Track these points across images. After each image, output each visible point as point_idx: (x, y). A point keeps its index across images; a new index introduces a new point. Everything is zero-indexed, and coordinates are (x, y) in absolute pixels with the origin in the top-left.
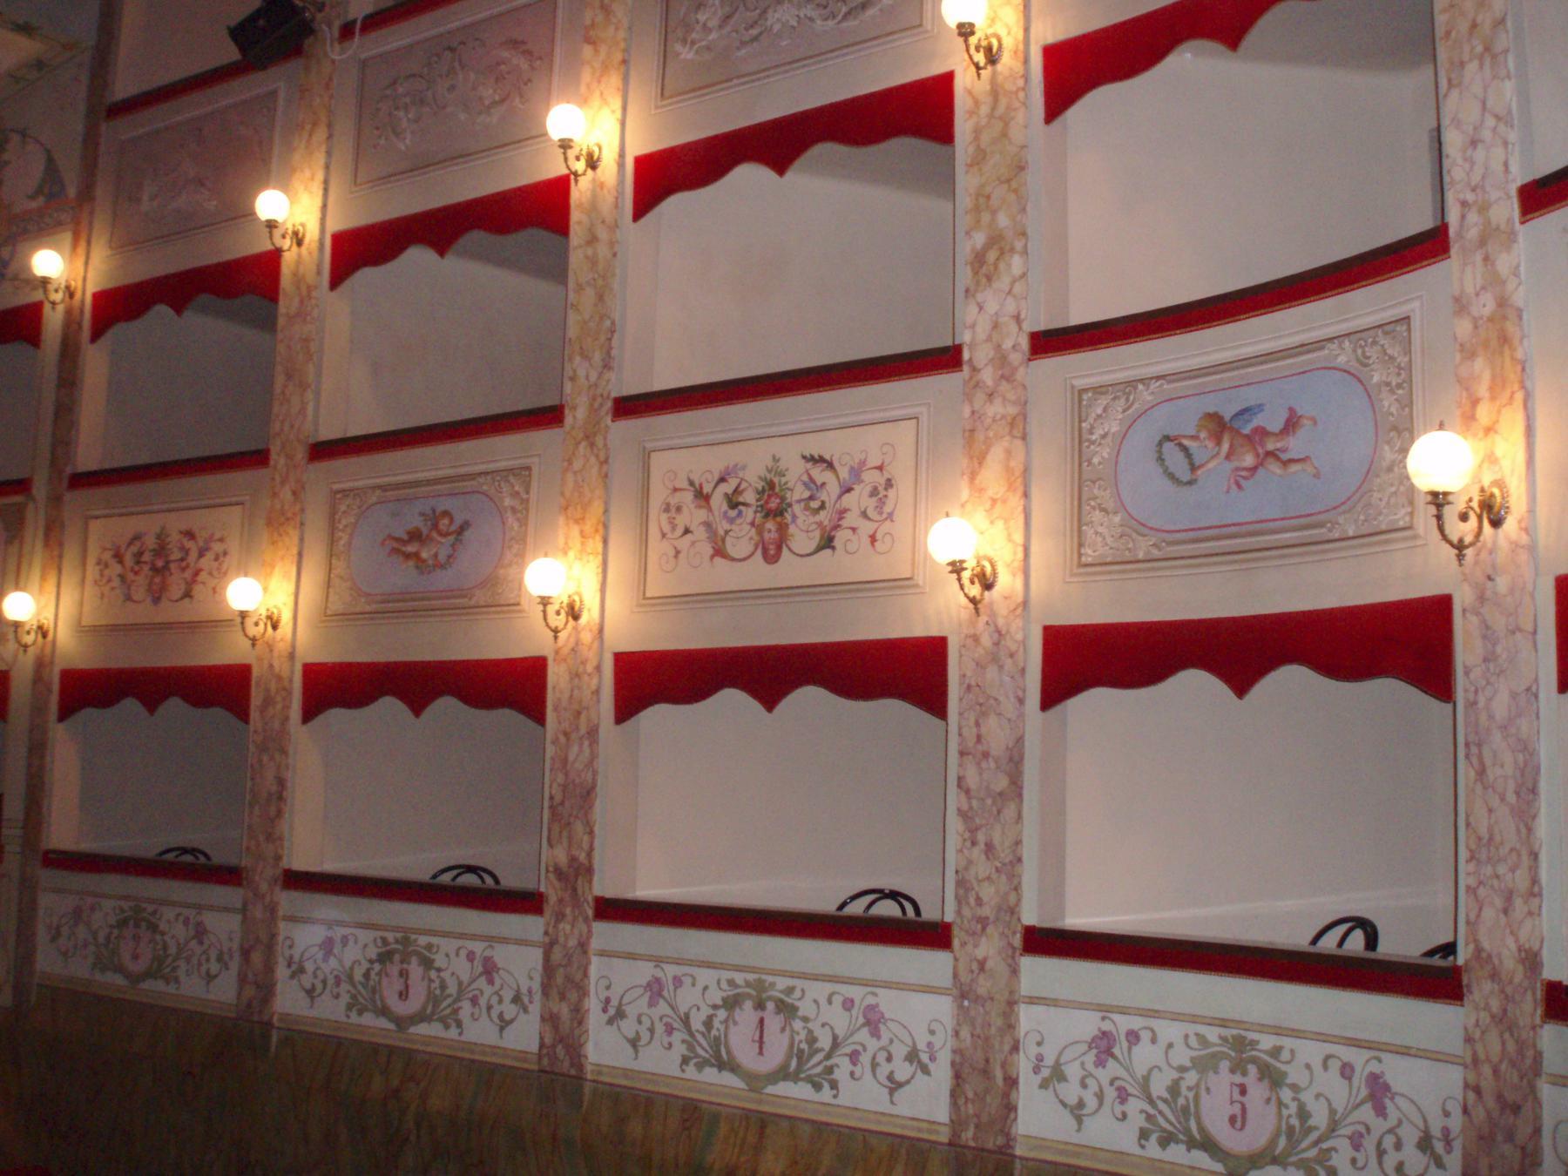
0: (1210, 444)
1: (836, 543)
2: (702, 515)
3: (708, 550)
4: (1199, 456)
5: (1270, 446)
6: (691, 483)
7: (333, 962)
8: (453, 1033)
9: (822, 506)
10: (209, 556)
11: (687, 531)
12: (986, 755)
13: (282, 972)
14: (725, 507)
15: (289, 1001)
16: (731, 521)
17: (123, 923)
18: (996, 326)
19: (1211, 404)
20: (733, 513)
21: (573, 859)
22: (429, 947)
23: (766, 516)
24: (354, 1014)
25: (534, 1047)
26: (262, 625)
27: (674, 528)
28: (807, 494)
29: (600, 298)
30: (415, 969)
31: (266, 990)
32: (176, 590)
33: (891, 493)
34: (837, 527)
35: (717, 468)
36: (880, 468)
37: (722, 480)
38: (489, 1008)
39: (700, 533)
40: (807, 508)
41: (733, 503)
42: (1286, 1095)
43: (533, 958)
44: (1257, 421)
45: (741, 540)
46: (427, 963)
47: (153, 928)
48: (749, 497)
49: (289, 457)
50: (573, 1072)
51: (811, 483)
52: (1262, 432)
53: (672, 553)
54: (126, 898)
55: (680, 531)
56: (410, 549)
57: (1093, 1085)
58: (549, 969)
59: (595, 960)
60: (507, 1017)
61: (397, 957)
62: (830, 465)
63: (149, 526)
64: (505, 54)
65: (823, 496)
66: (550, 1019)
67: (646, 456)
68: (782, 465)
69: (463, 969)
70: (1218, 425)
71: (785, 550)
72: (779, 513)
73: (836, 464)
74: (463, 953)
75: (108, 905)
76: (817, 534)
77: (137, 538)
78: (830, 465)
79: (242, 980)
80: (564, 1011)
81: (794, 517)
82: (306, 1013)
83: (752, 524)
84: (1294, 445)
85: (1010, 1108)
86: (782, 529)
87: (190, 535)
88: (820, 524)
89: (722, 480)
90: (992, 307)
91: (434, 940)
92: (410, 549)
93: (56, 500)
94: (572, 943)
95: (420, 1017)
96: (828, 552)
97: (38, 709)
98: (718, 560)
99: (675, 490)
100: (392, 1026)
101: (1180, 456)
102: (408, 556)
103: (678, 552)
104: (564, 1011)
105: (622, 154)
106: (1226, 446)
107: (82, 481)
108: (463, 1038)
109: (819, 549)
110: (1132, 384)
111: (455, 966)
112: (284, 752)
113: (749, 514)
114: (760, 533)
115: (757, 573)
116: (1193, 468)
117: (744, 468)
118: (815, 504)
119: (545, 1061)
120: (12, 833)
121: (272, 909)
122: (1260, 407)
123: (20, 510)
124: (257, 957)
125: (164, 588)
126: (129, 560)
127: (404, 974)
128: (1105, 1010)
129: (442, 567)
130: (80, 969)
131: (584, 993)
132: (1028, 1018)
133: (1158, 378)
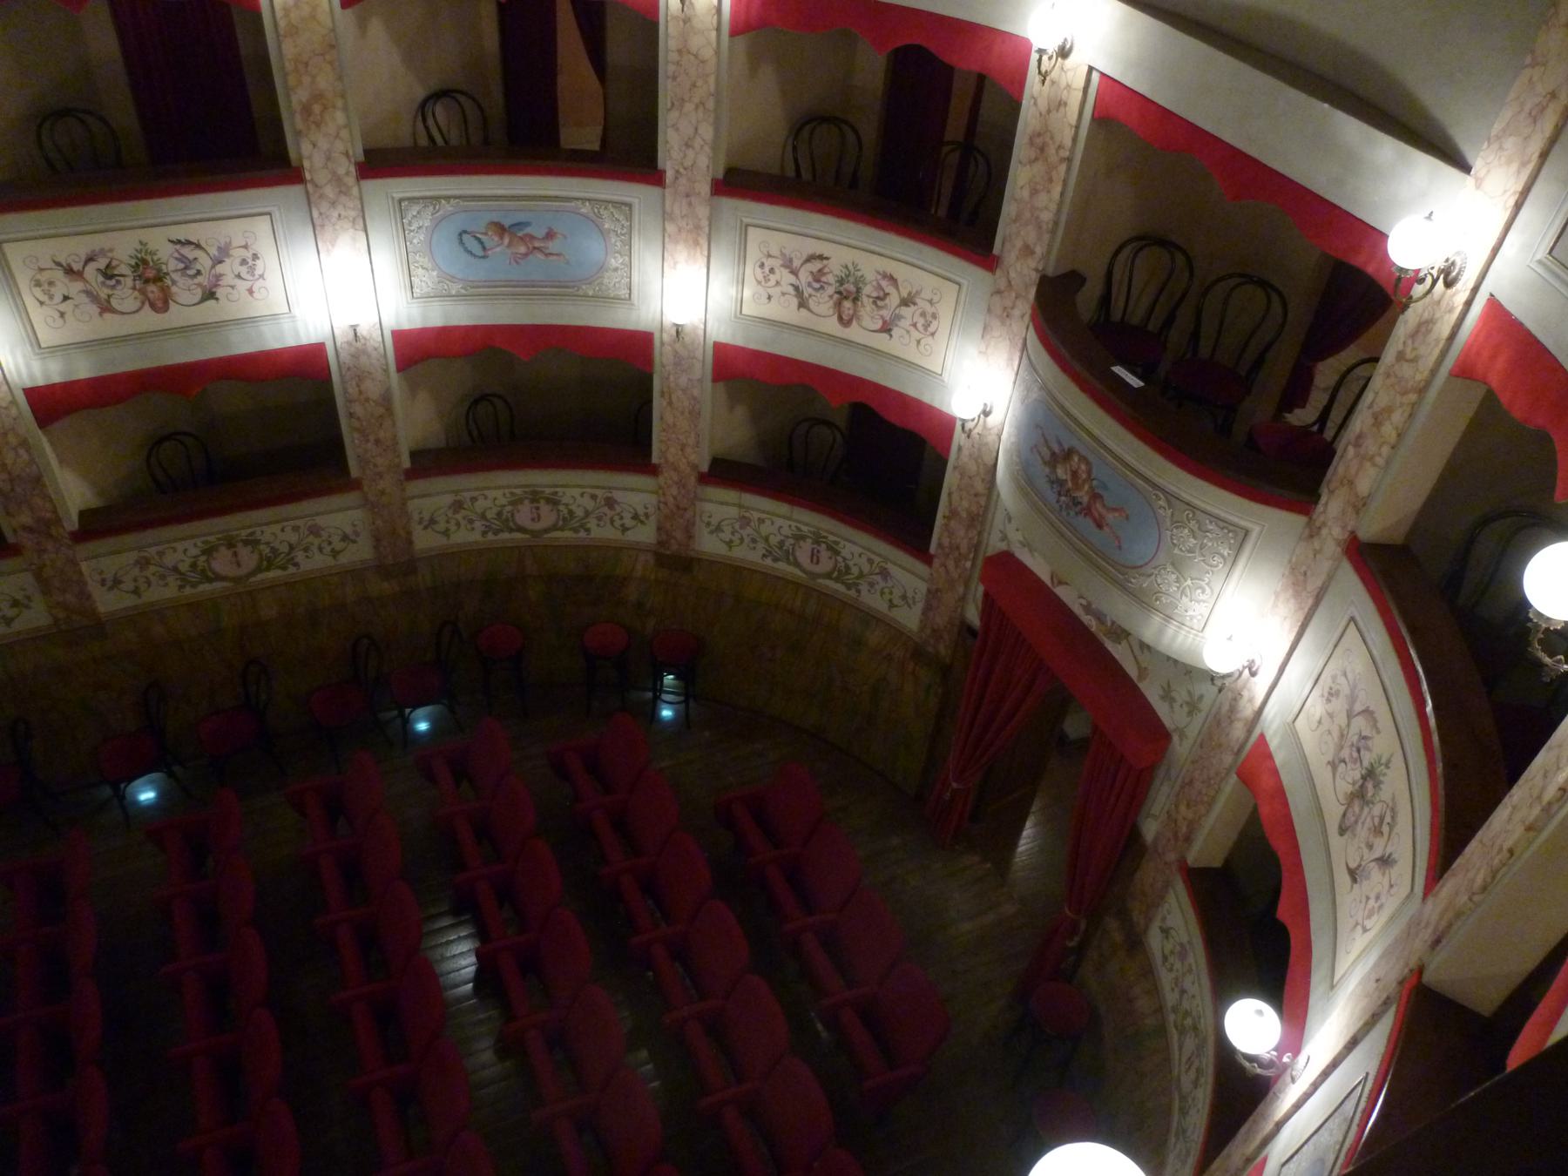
0: (496, 239)
2: (79, 285)
3: (94, 309)
4: (487, 245)
5: (537, 244)
6: (59, 264)
9: (199, 272)
11: (66, 298)
12: (367, 400)
14: (101, 279)
16: (113, 287)
18: (329, 158)
19: (495, 217)
23: (147, 281)
27: (51, 297)
34: (217, 286)
35: (83, 253)
36: (246, 247)
37: (90, 259)
39: (84, 299)
41: (108, 274)
42: (561, 508)
44: (528, 230)
45: (125, 297)
51: (182, 259)
52: (532, 238)
53: (57, 315)
55: (58, 298)
57: (453, 522)
62: (198, 246)
65: (198, 267)
68: (151, 247)
70: (500, 229)
72: (159, 278)
73: (203, 244)
76: (199, 292)
78: (198, 246)
81: (174, 282)
83: (134, 288)
84: (553, 246)
85: (410, 542)
88: (199, 285)
89: (90, 259)
90: (323, 144)
96: (211, 303)
98: (108, 316)
99: (41, 270)
101: (475, 243)
103: (62, 315)
104: (70, 598)
106: (506, 241)
109: (203, 300)
110: (438, 198)
114: (143, 292)
115: (149, 320)
116: (484, 248)
117: (111, 250)
122: (527, 224)
128: (456, 492)
132: (412, 505)
133: (459, 197)
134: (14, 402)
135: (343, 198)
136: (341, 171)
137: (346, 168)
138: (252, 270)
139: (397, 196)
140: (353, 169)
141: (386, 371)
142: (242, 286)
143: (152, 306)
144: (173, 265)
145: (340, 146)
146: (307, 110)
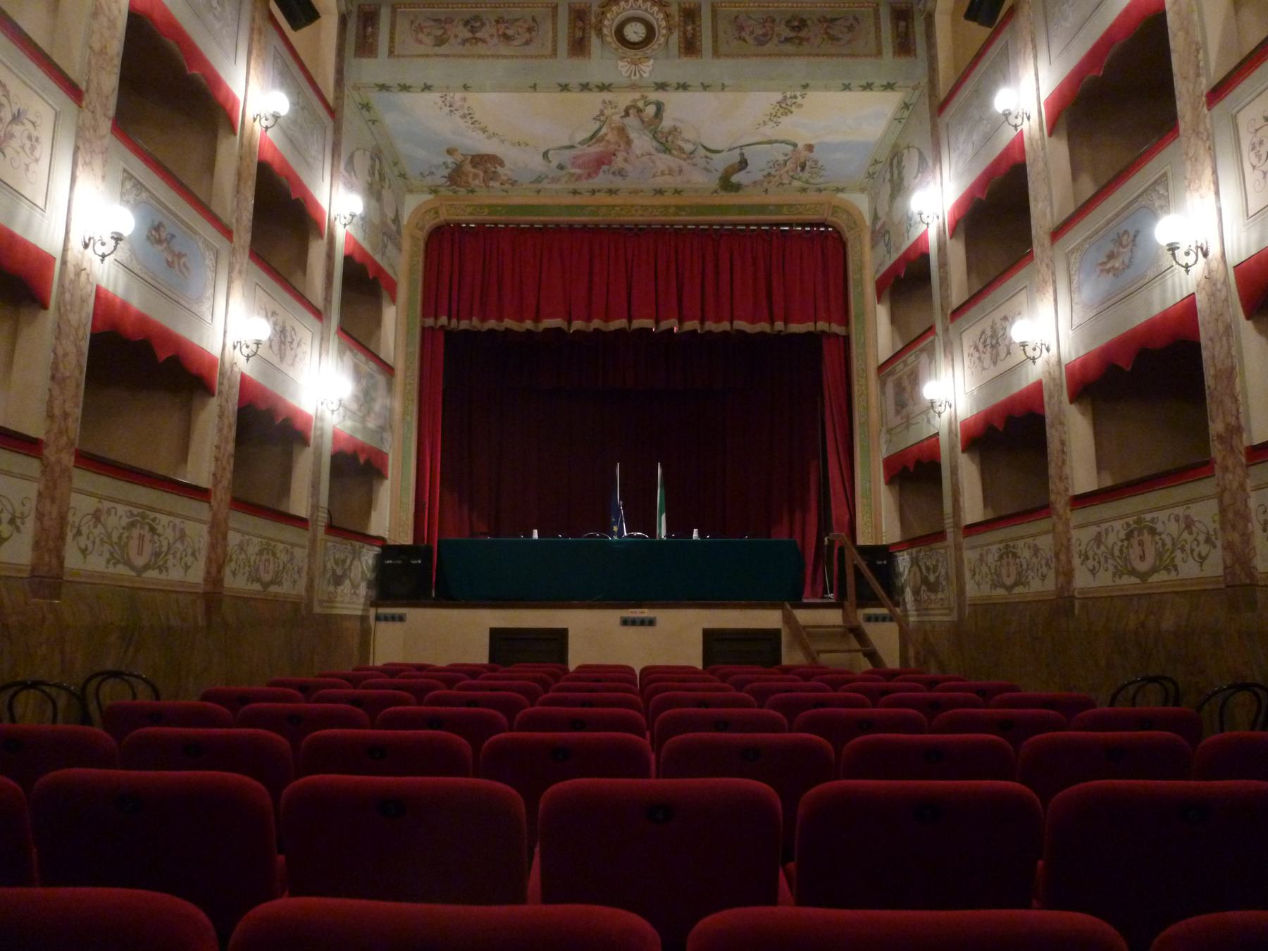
7: (1102, 547)
8: (1173, 575)
13: (1076, 561)
15: (1082, 580)
17: (1001, 558)
21: (1227, 425)
22: (1153, 520)
24: (1117, 579)
25: (1220, 571)
26: (1038, 350)
29: (1187, 33)
30: (1147, 537)
31: (1068, 575)
32: (1003, 354)
38: (1192, 551)
43: (1213, 506)
46: (1153, 531)
47: (1015, 555)
49: (1043, 246)
50: (1248, 581)
54: (1001, 542)
56: (1109, 266)
58: (1223, 511)
59: (1253, 494)
60: (1204, 554)
61: (1136, 533)
63: (985, 324)
66: (1229, 546)
67: (1234, 118)
69: (1173, 528)
74: (1172, 518)
75: (994, 548)
77: (983, 333)
79: (1057, 573)
80: (1235, 537)
82: (1093, 584)
91: (1154, 515)
92: (1109, 266)
93: (946, 330)
94: (1235, 484)
95: (1154, 570)
100: (1138, 581)
102: (1108, 271)
104: (1235, 537)
107: (957, 313)
108: (1180, 576)
111: (1169, 526)
112: (1062, 423)
119: (1229, 578)
120: (949, 522)
121: (1067, 524)
123: (933, 342)
124: (1063, 557)
125: (998, 354)
126: (981, 347)
127: (1141, 544)
129: (1128, 267)
130: (986, 590)
131: (1246, 518)
134: (1226, 282)
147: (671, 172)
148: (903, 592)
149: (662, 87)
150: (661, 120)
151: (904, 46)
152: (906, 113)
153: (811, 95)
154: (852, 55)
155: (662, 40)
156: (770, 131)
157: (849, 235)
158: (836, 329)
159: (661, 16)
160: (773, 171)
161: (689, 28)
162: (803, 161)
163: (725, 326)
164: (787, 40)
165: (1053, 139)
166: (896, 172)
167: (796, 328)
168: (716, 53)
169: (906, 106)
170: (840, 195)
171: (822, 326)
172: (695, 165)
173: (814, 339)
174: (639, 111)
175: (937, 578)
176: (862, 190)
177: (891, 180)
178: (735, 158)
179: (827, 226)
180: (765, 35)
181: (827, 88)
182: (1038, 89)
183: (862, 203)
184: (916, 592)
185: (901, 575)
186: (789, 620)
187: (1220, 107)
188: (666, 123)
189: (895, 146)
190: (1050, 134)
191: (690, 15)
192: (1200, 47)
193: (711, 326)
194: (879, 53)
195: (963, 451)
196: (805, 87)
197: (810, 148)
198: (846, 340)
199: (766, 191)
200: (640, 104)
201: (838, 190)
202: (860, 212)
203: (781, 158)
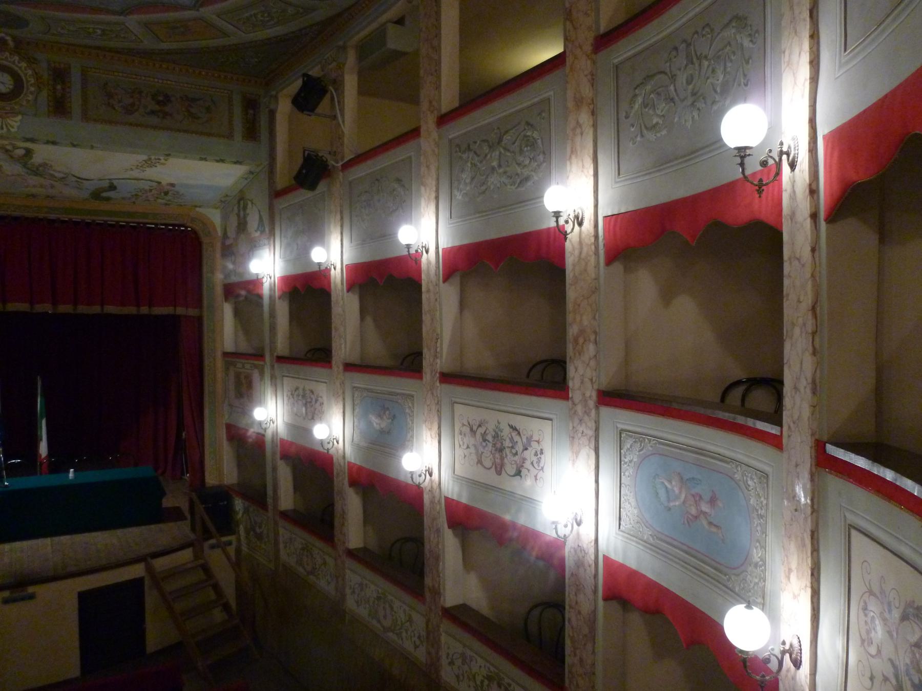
1: (522, 474)
10: (318, 403)
12: (579, 613)
16: (484, 447)
20: (484, 444)
28: (510, 445)
33: (543, 456)
37: (480, 426)
40: (511, 452)
48: (489, 438)
51: (512, 439)
64: (396, 186)
71: (503, 472)
72: (501, 450)
78: (519, 433)
86: (502, 459)
87: (312, 392)
89: (480, 426)
97: (274, 453)
105: (437, 248)
113: (490, 445)
114: (494, 457)
118: (514, 451)
134: (439, 501)
135: (586, 418)
136: (588, 394)
137: (591, 393)
138: (539, 461)
139: (621, 426)
140: (594, 394)
141: (595, 591)
142: (533, 471)
143: (496, 468)
144: (507, 443)
145: (589, 373)
146: (576, 340)
147: (41, 186)
148: (238, 526)
149: (32, 140)
150: (31, 158)
151: (251, 133)
152: (251, 176)
153: (172, 160)
154: (209, 135)
155: (31, 97)
156: (136, 174)
157: (205, 240)
158: (192, 312)
159: (30, 72)
160: (140, 194)
161: (59, 87)
162: (166, 191)
163: (96, 309)
164: (153, 112)
165: (350, 294)
166: (242, 213)
167: (158, 311)
168: (85, 117)
169: (251, 173)
170: (197, 209)
171: (180, 311)
172: (66, 185)
173: (175, 318)
174: (7, 151)
175: (262, 533)
176: (217, 208)
177: (238, 215)
178: (106, 184)
179: (186, 227)
180: (133, 105)
181: (186, 158)
182: (342, 252)
183: (215, 217)
184: (247, 532)
185: (238, 514)
186: (150, 570)
187: (447, 388)
188: (37, 159)
189: (241, 191)
190: (348, 290)
191: (60, 75)
192: (438, 338)
193: (82, 309)
194: (230, 136)
195: (281, 459)
196: (168, 155)
197: (173, 185)
198: (200, 319)
199: (134, 203)
200: (9, 148)
201: (196, 206)
202: (214, 226)
203: (147, 188)
